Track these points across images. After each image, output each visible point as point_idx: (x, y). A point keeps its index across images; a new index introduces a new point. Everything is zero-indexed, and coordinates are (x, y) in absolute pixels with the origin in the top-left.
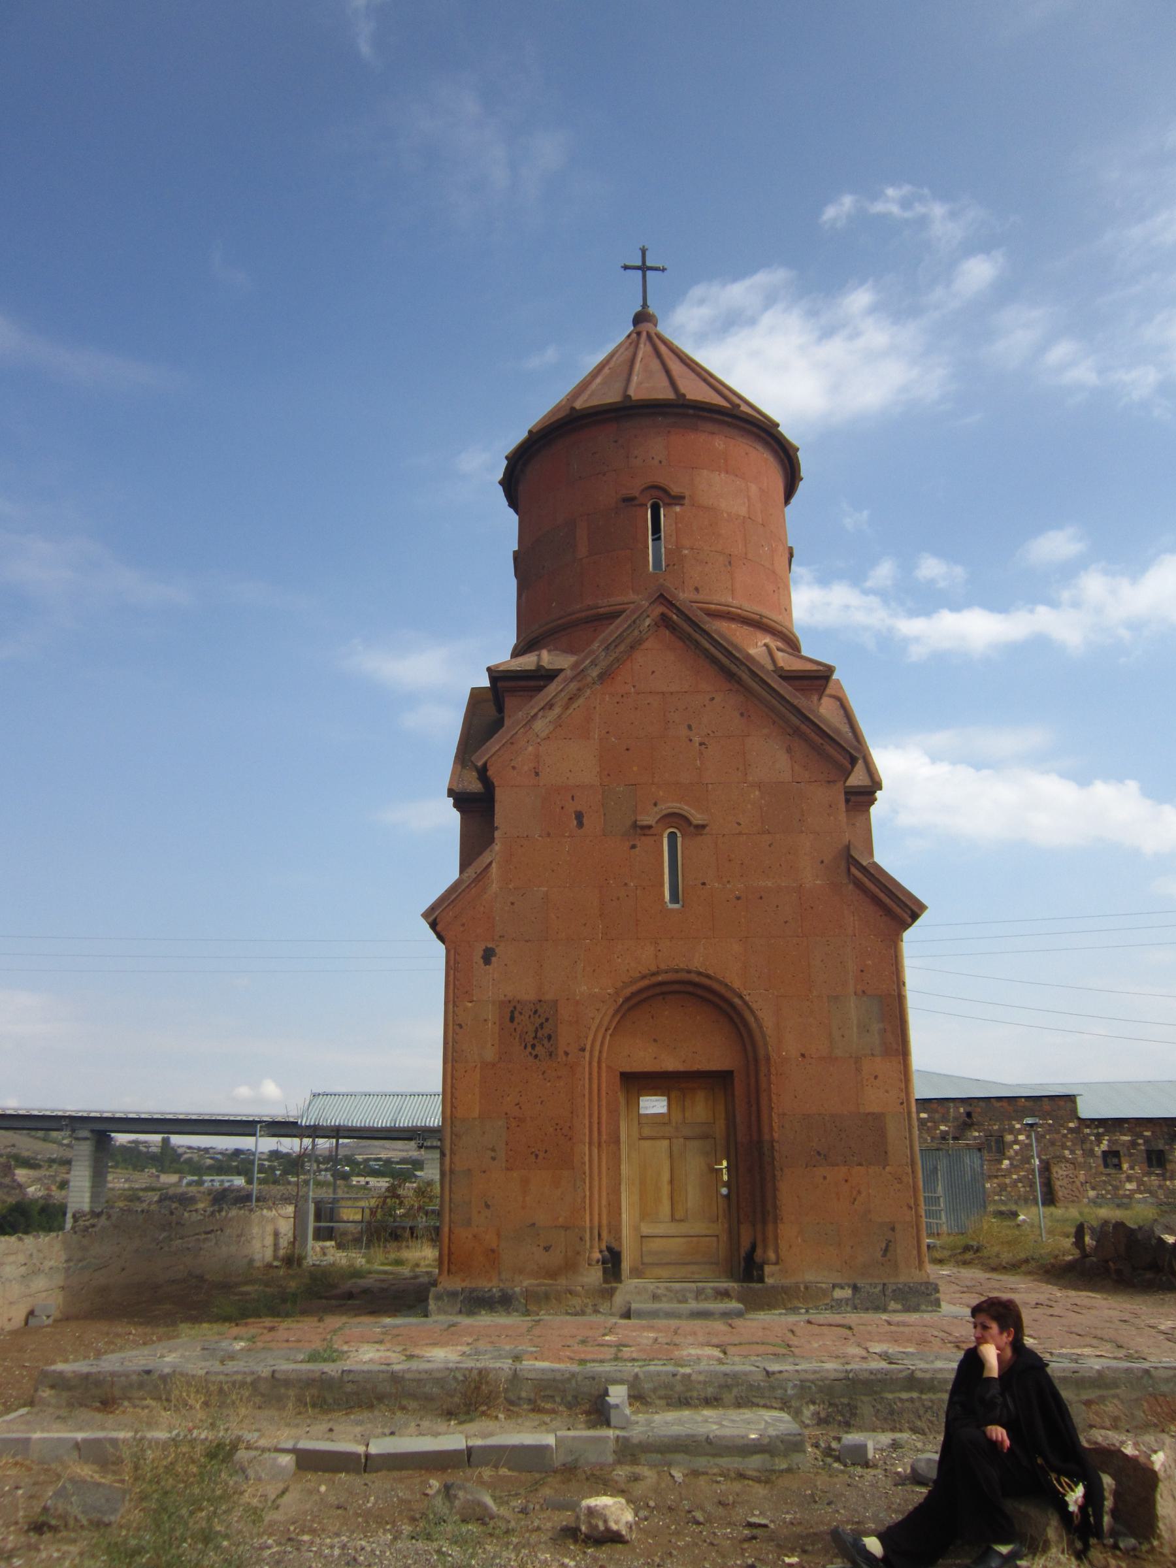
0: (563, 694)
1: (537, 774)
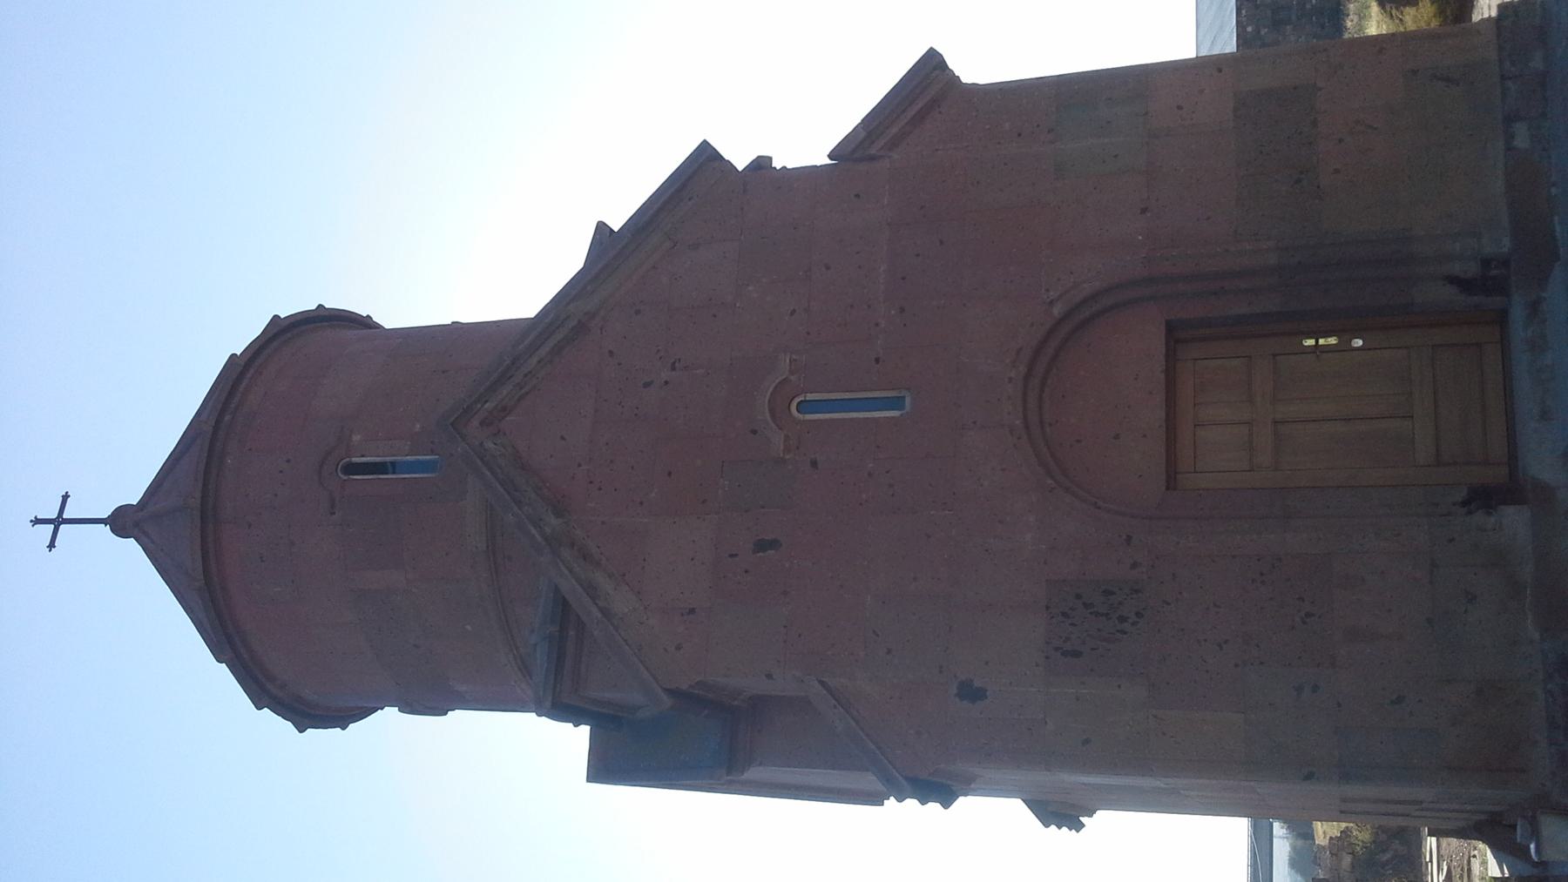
1: (692, 611)
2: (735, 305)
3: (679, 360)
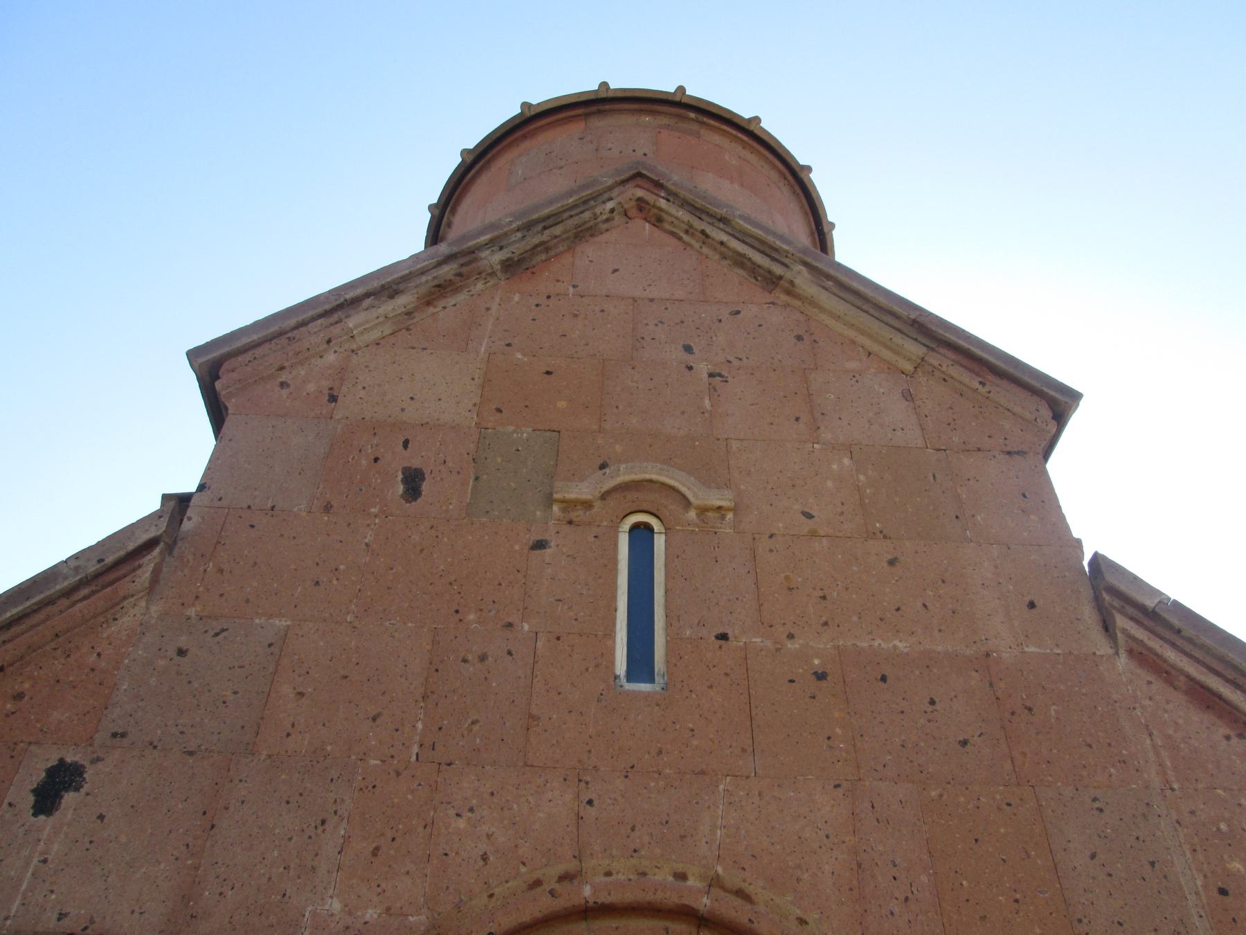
0: (424, 279)
1: (333, 399)
2: (817, 443)
3: (726, 381)
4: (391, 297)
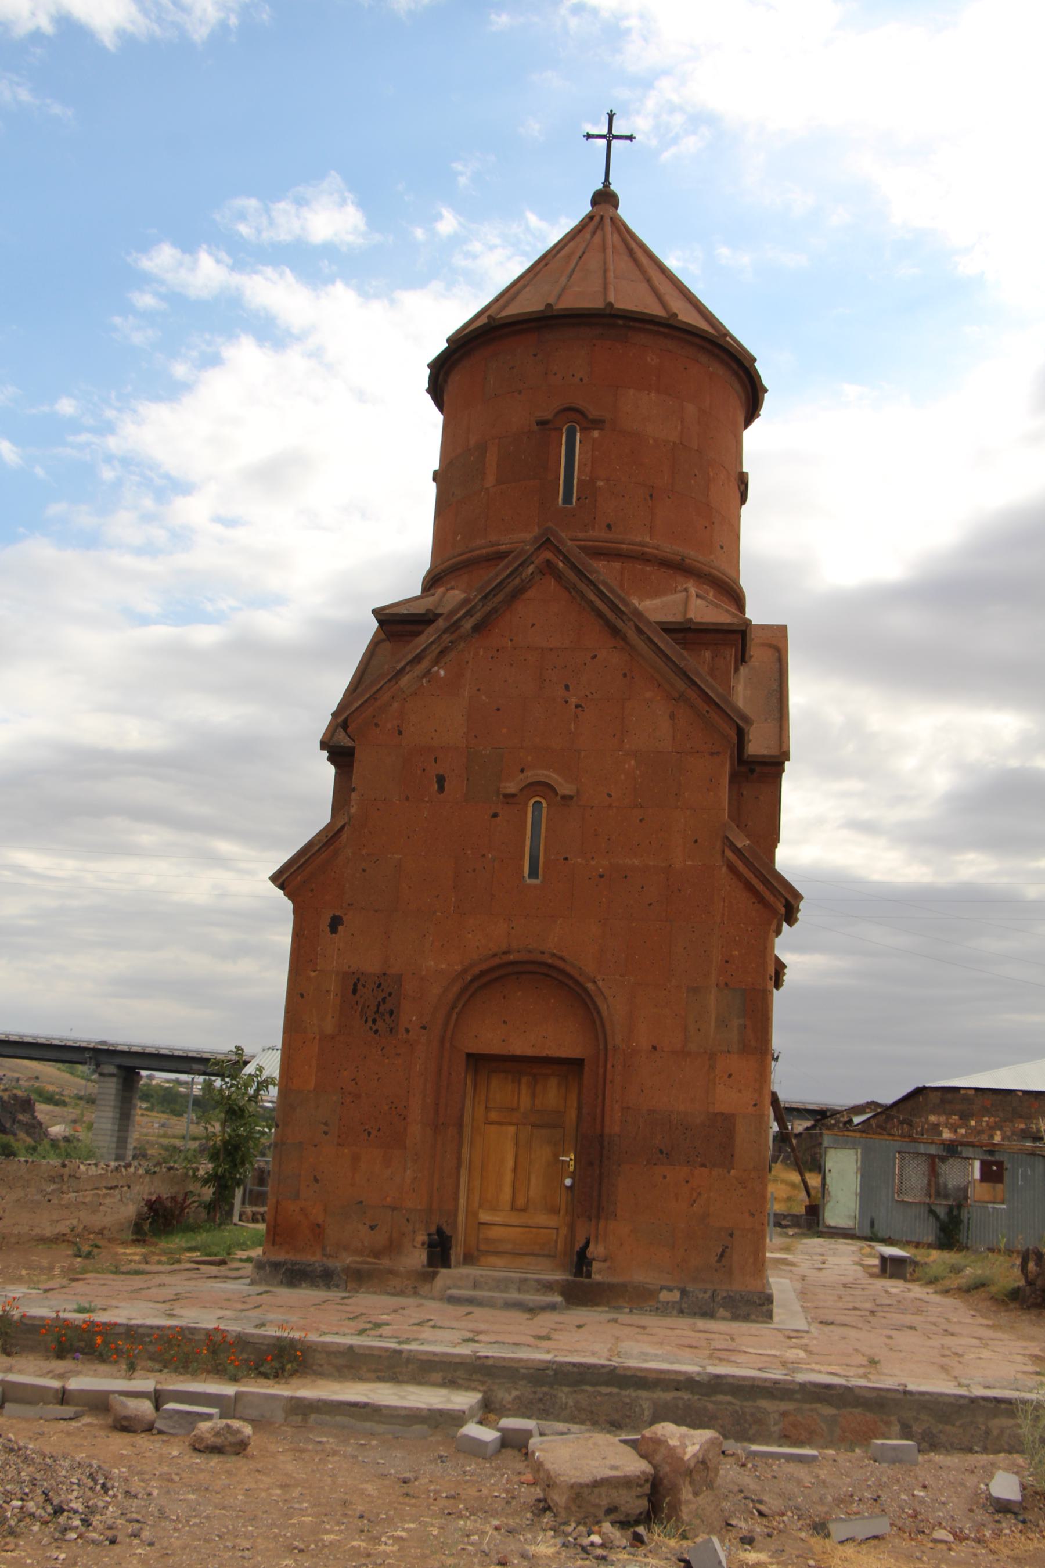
0: (434, 647)
1: (400, 733)
4: (419, 662)
